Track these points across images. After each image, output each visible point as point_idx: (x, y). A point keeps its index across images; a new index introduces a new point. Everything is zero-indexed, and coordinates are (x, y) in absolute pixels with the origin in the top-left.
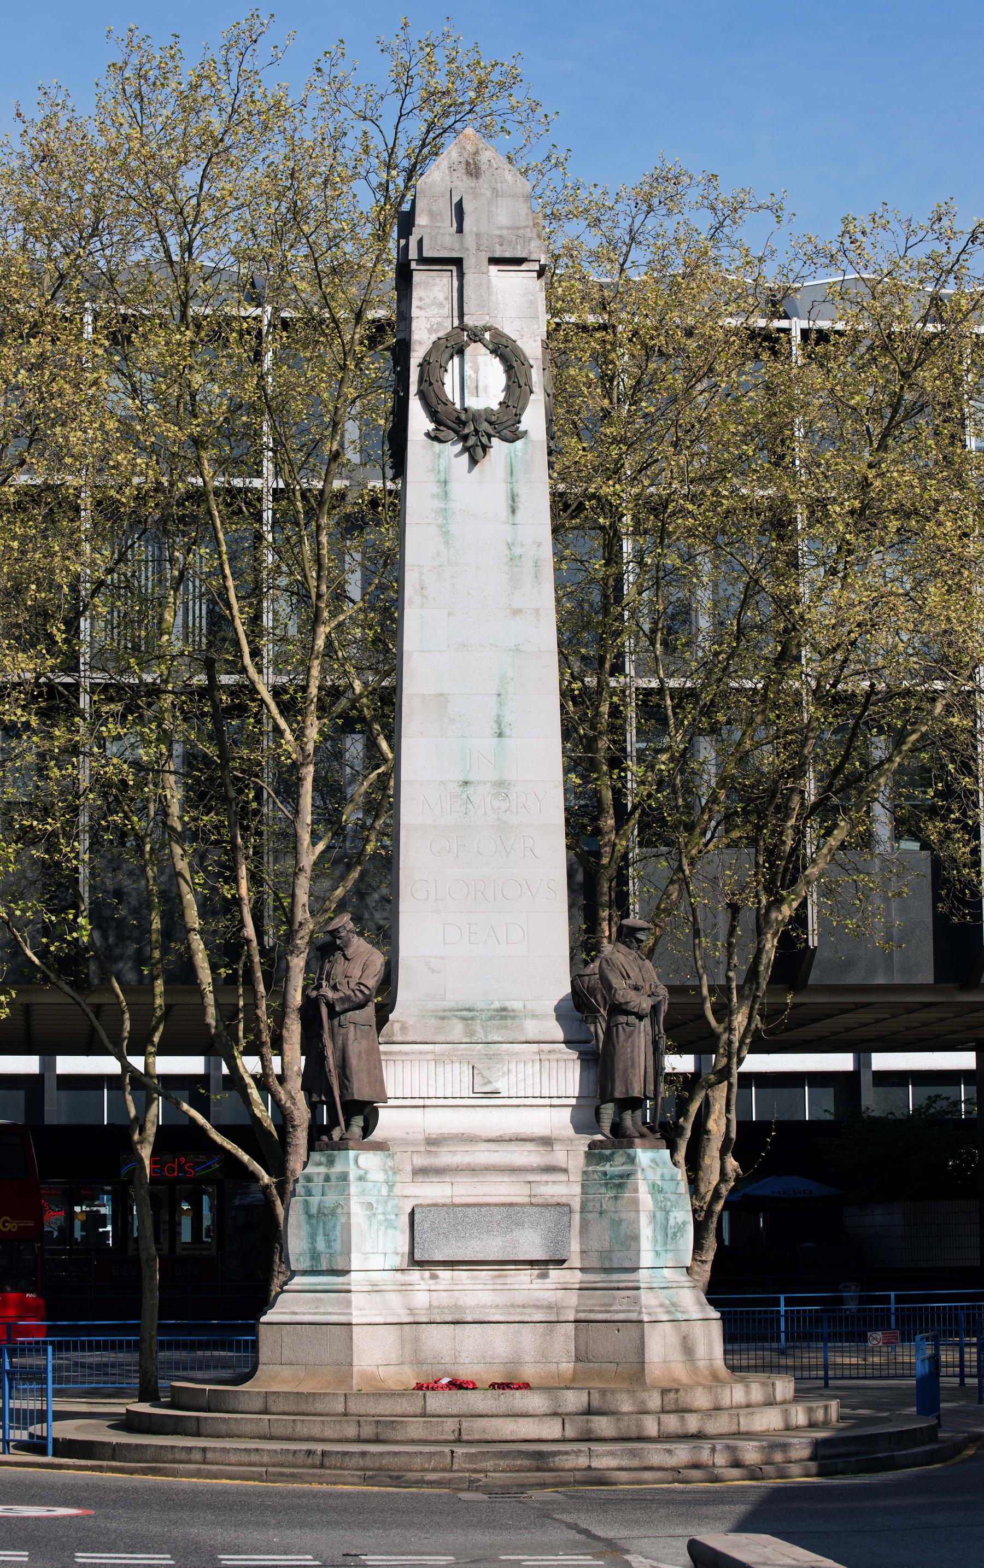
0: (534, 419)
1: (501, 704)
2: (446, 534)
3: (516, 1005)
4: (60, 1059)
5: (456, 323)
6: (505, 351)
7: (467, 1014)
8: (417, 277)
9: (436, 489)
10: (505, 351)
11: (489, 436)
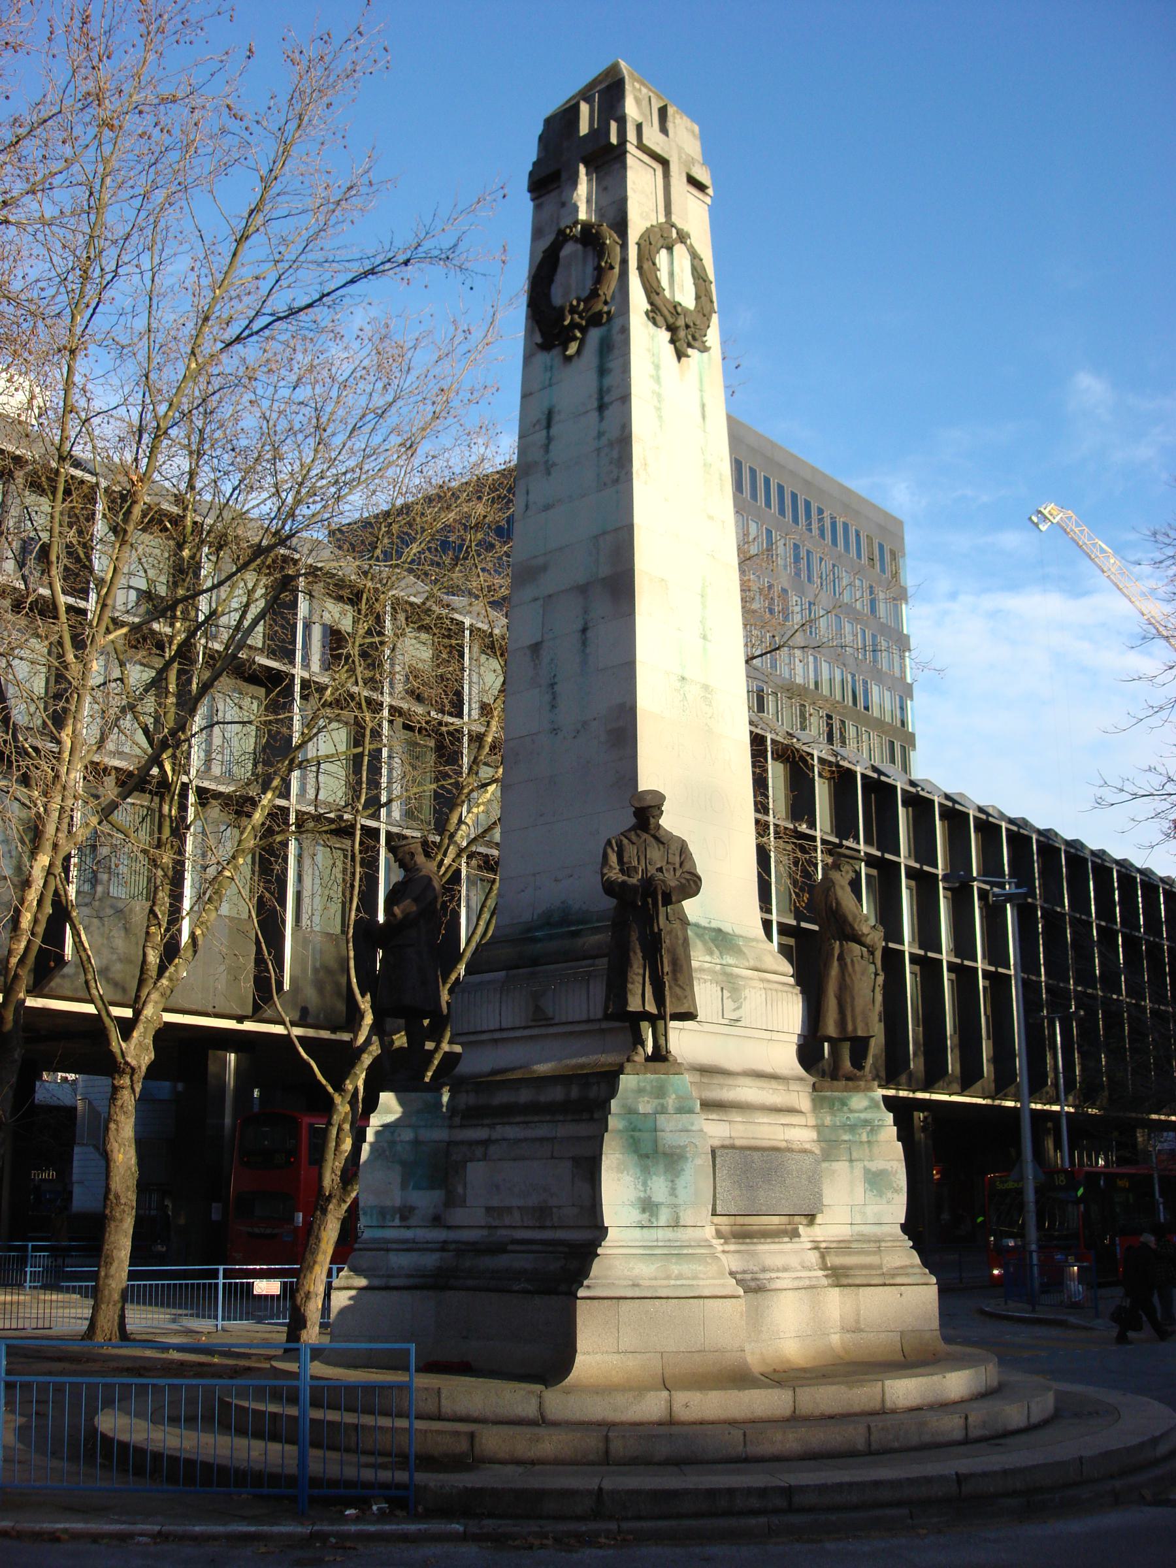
0: (713, 336)
5: (662, 219)
8: (630, 160)
9: (653, 373)
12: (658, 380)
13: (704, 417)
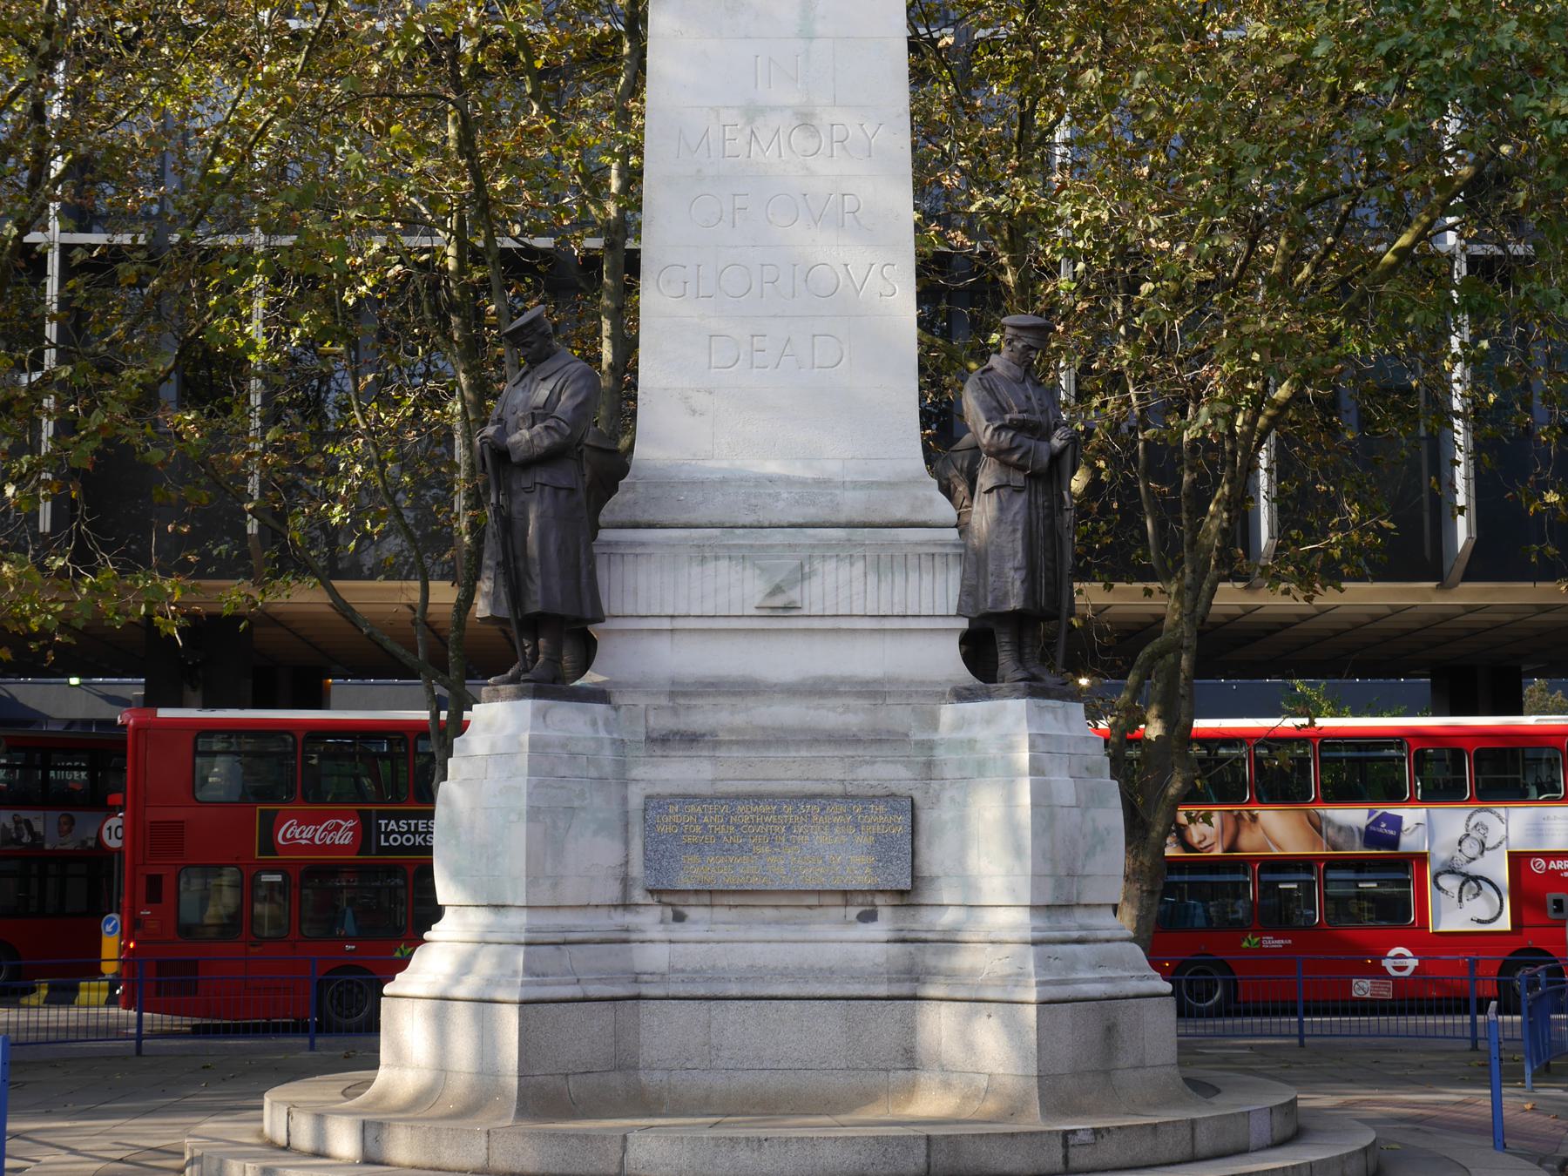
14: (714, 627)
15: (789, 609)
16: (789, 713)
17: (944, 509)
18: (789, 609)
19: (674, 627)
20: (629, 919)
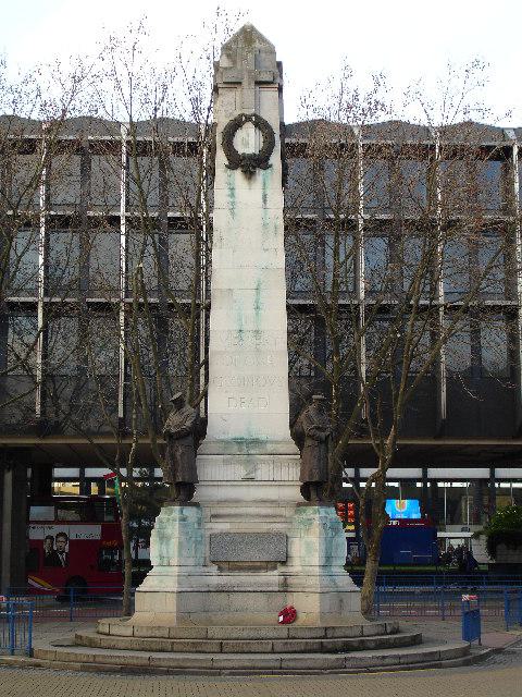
0: (275, 159)
1: (258, 294)
2: (233, 214)
3: (263, 437)
4: (11, 473)
6: (261, 124)
7: (239, 442)
9: (228, 192)
10: (261, 124)
11: (254, 168)
12: (232, 195)
13: (265, 201)
14: (231, 483)
15: (252, 479)
16: (252, 510)
17: (297, 450)
18: (252, 479)
19: (217, 484)
20: (206, 569)
